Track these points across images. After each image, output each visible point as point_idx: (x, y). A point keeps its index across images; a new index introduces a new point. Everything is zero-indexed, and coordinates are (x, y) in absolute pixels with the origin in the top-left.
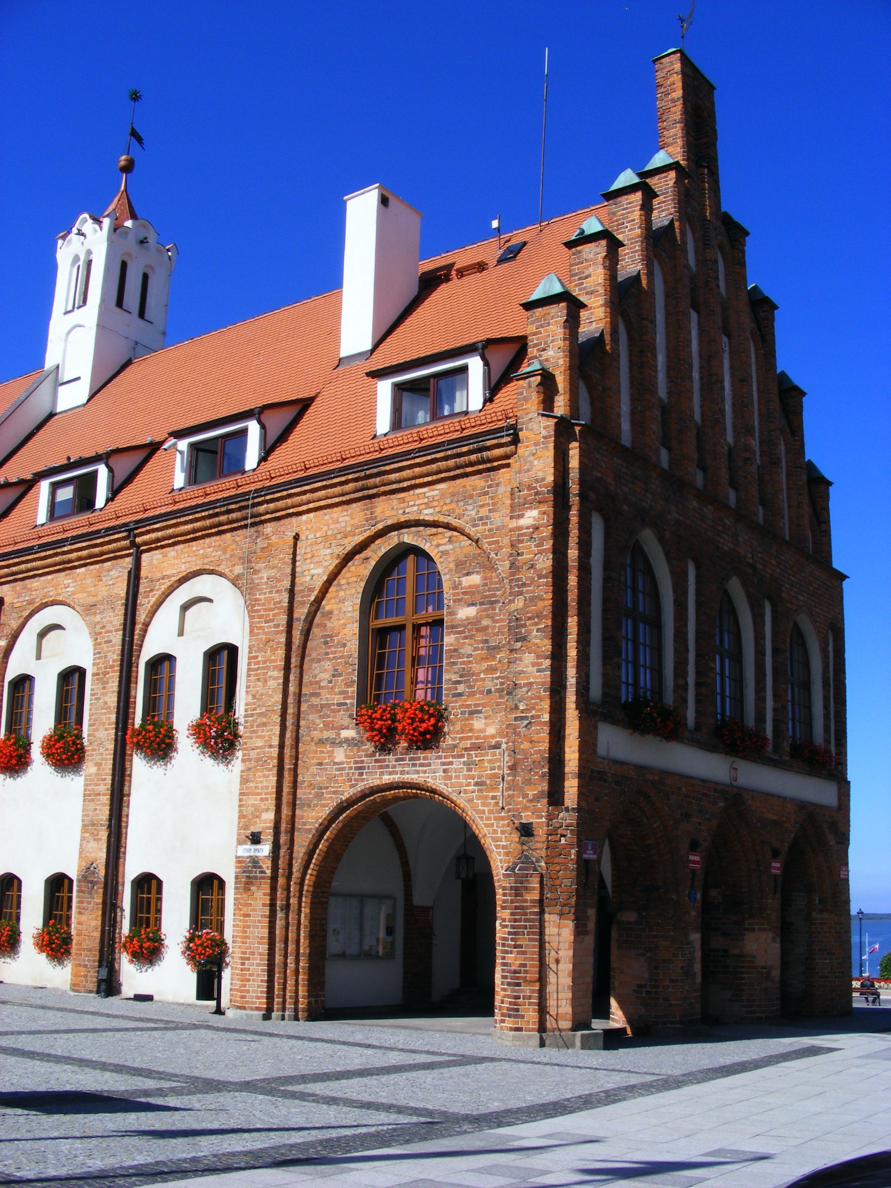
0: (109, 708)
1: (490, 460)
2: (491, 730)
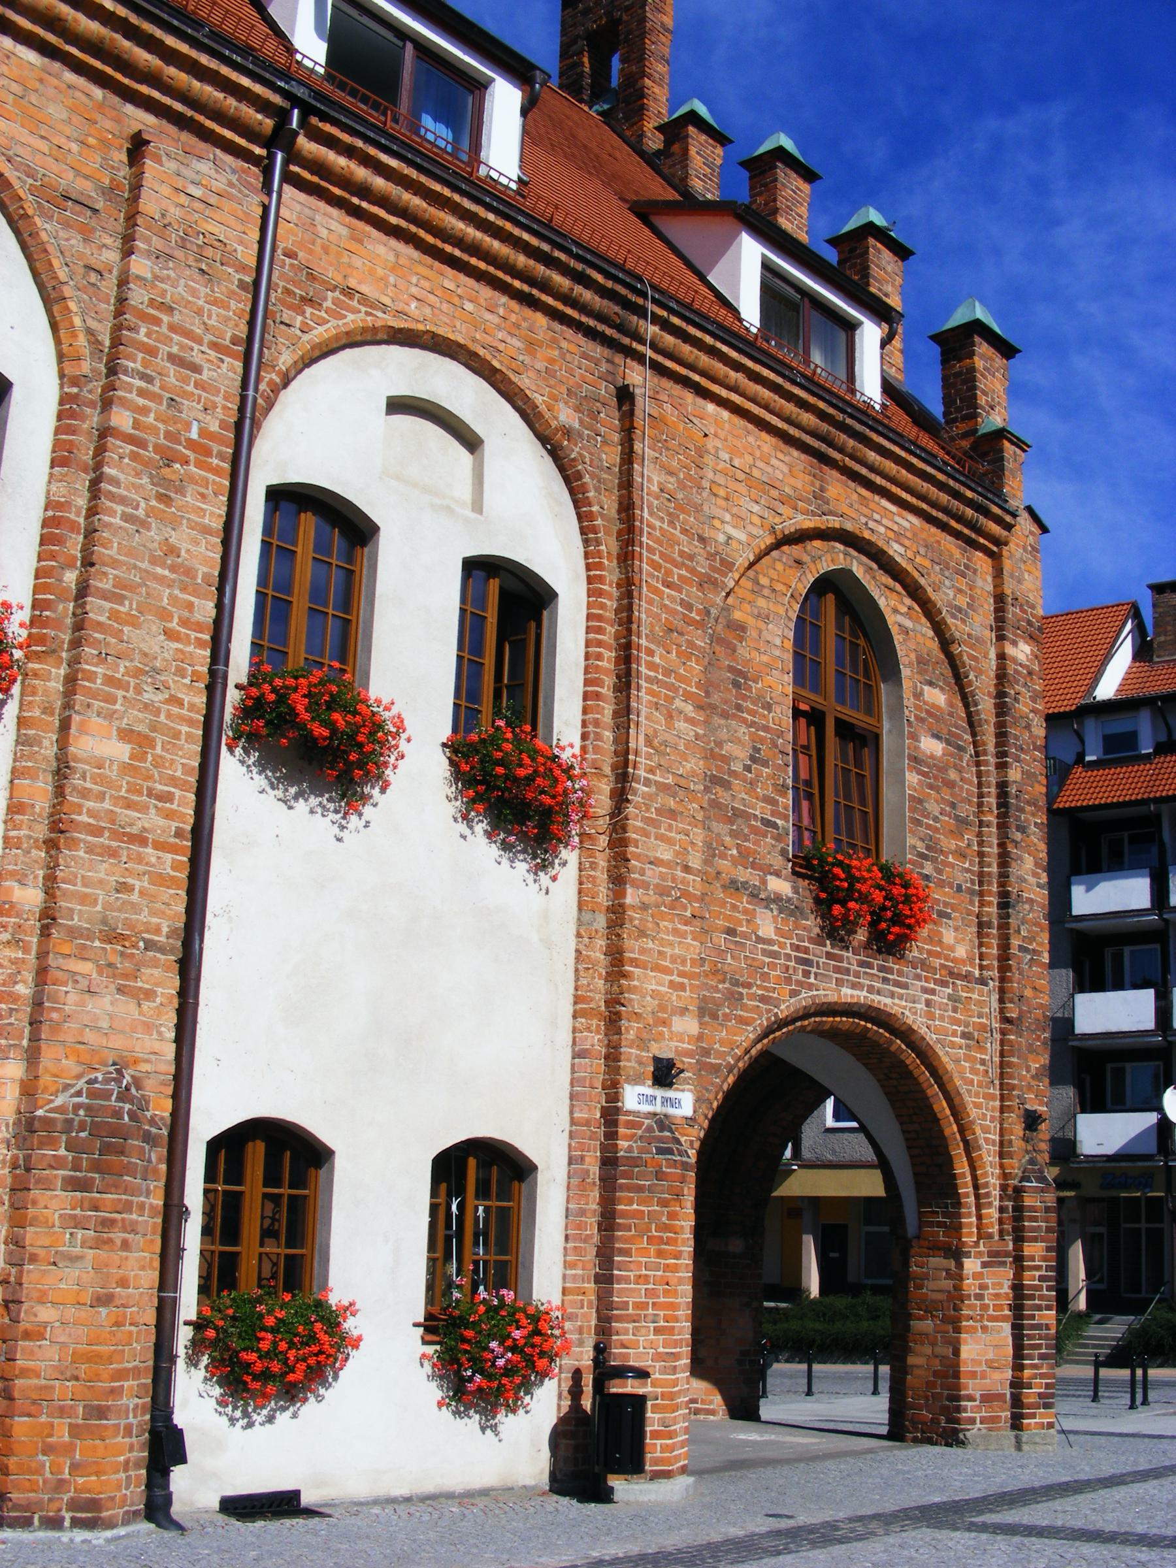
0: (189, 572)
1: (979, 531)
2: (961, 952)
